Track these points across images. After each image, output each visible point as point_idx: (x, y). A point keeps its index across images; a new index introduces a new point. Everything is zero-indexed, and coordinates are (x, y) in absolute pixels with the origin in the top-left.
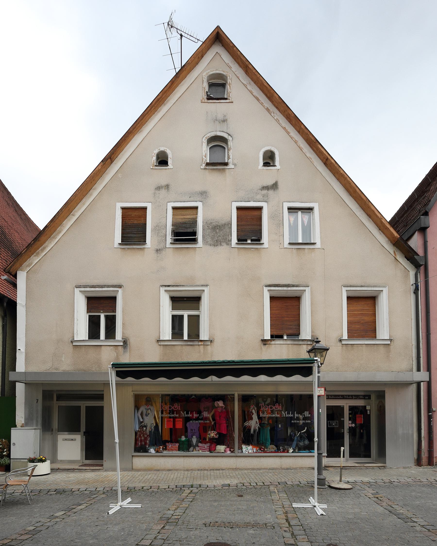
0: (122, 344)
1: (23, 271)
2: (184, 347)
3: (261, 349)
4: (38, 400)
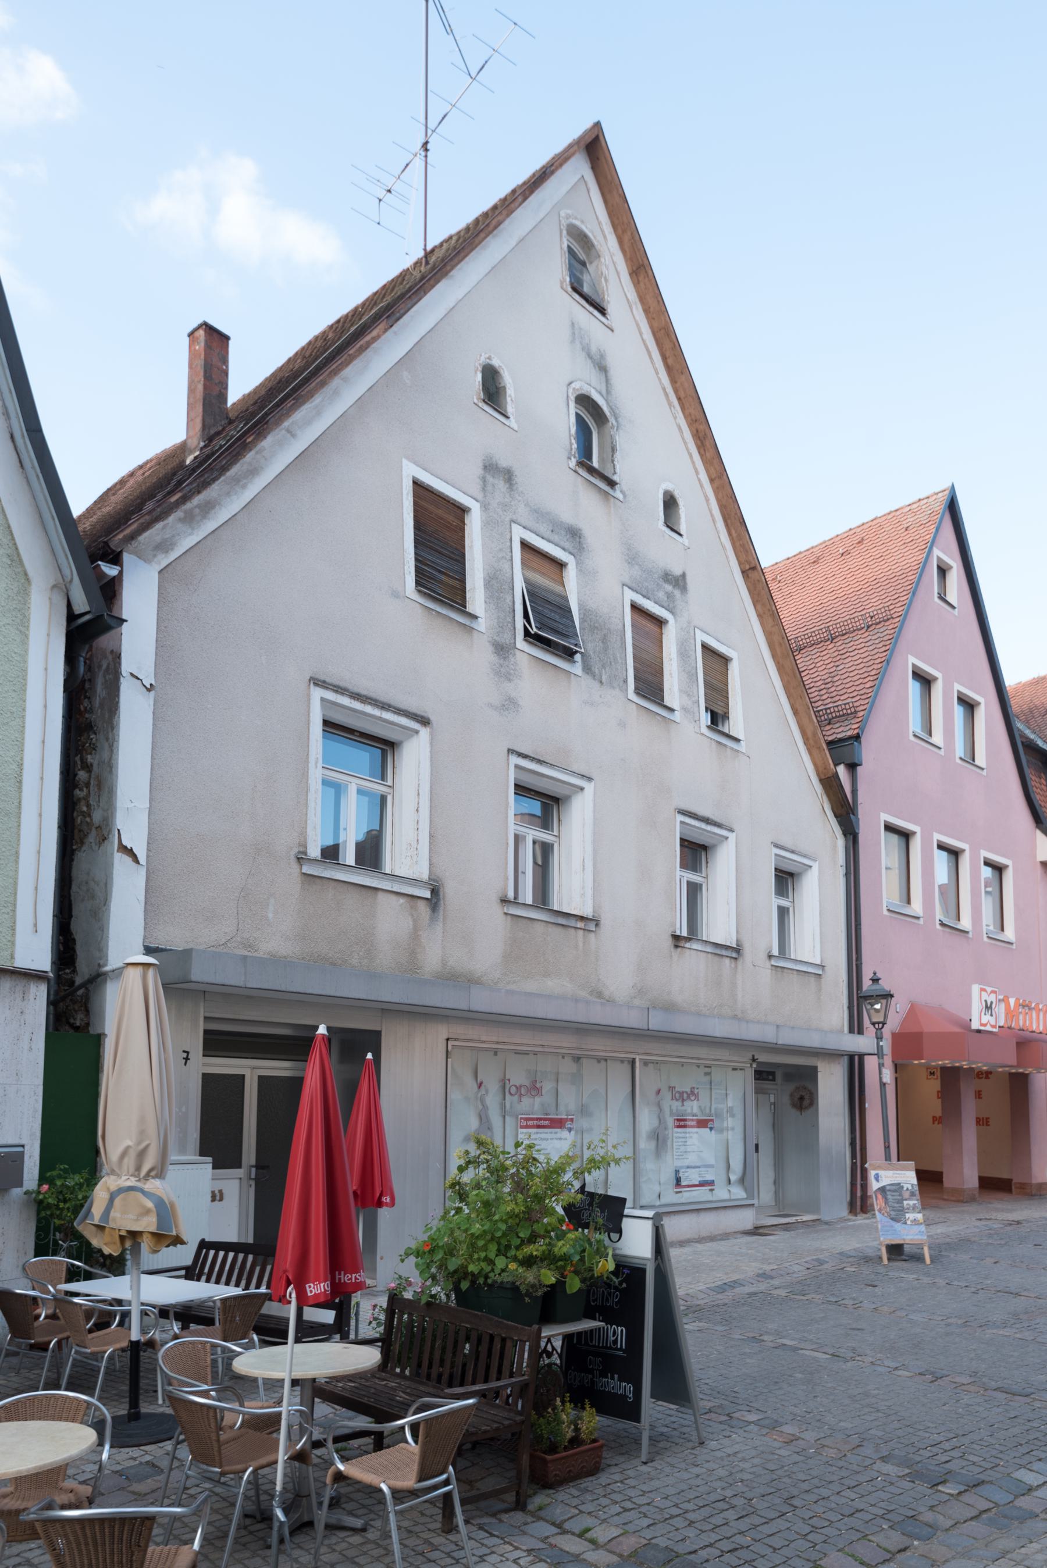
0: (427, 894)
1: (145, 561)
2: (552, 929)
3: (671, 956)
4: (188, 1053)
